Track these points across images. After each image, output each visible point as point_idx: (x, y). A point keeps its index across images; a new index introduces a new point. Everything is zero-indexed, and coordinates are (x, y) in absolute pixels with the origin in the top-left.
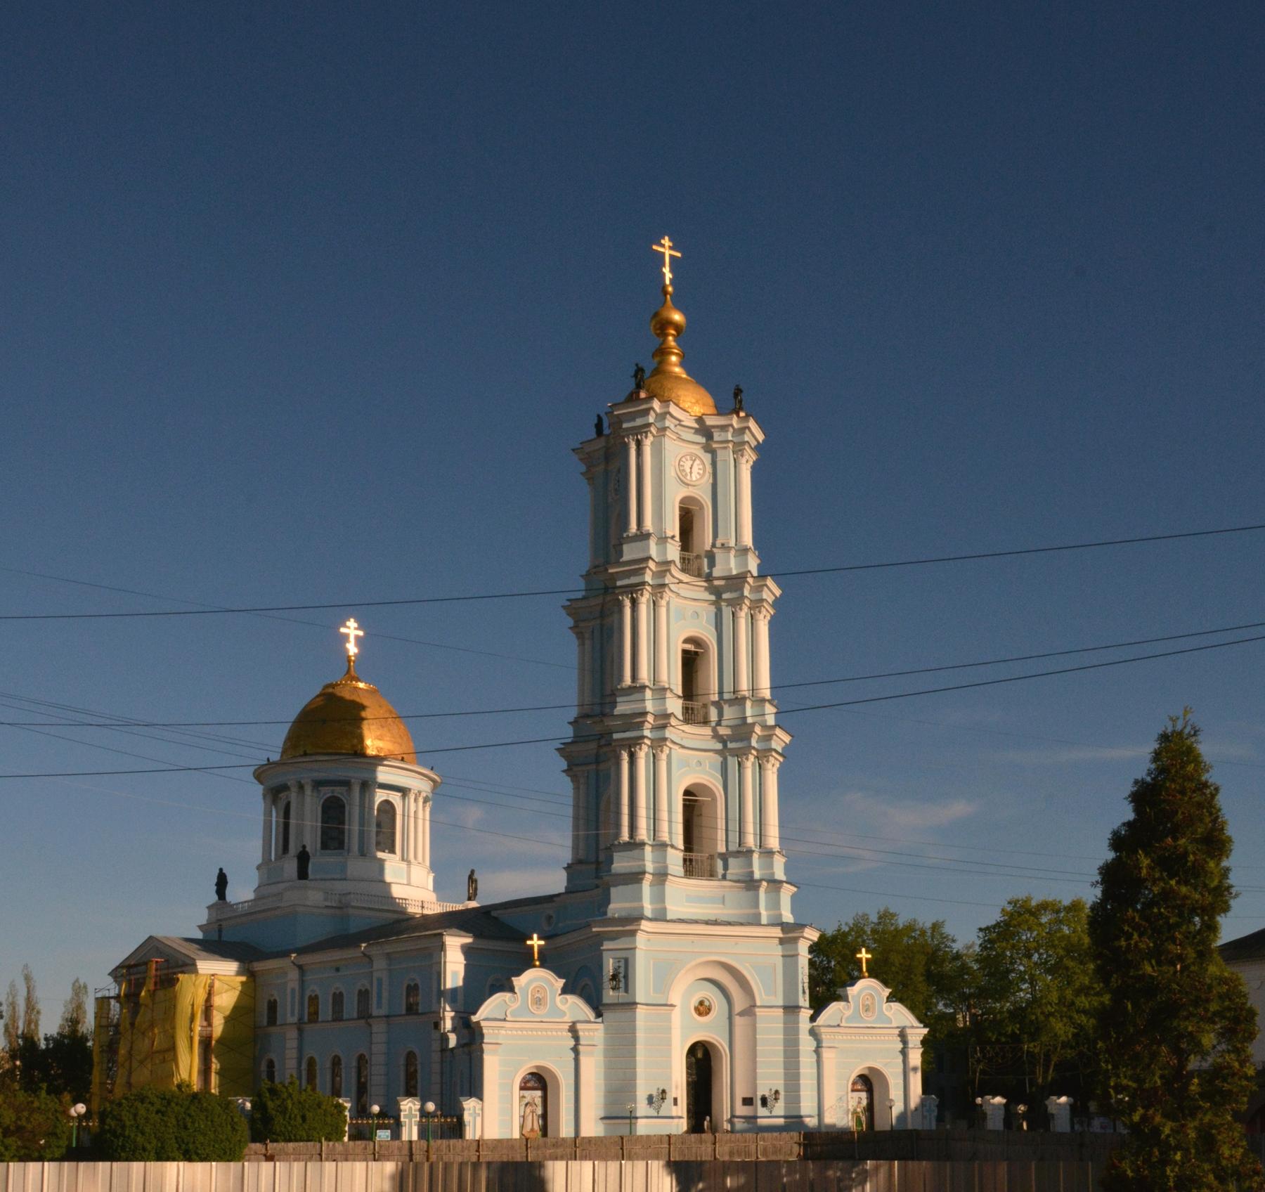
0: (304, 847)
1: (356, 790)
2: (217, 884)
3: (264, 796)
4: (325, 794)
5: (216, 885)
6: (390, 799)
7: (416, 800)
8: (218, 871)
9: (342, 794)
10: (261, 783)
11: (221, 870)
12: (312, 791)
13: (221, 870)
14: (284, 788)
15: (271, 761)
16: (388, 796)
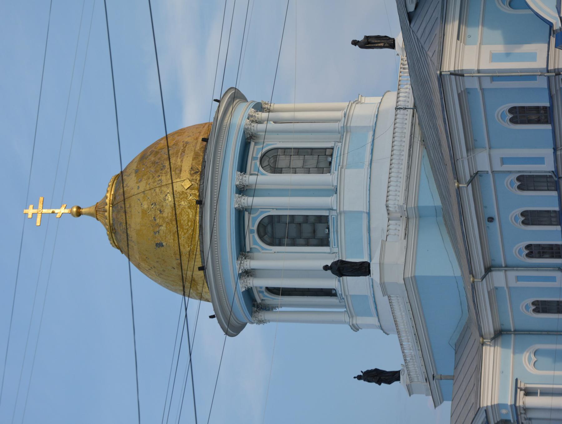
0: (326, 268)
1: (247, 201)
2: (379, 383)
3: (261, 322)
4: (255, 243)
5: (380, 384)
6: (259, 156)
7: (259, 122)
8: (362, 381)
9: (255, 219)
10: (243, 326)
11: (359, 378)
12: (251, 258)
13: (359, 378)
14: (249, 293)
15: (213, 313)
16: (257, 158)
